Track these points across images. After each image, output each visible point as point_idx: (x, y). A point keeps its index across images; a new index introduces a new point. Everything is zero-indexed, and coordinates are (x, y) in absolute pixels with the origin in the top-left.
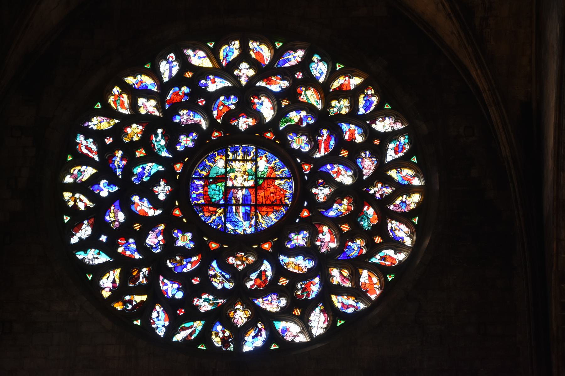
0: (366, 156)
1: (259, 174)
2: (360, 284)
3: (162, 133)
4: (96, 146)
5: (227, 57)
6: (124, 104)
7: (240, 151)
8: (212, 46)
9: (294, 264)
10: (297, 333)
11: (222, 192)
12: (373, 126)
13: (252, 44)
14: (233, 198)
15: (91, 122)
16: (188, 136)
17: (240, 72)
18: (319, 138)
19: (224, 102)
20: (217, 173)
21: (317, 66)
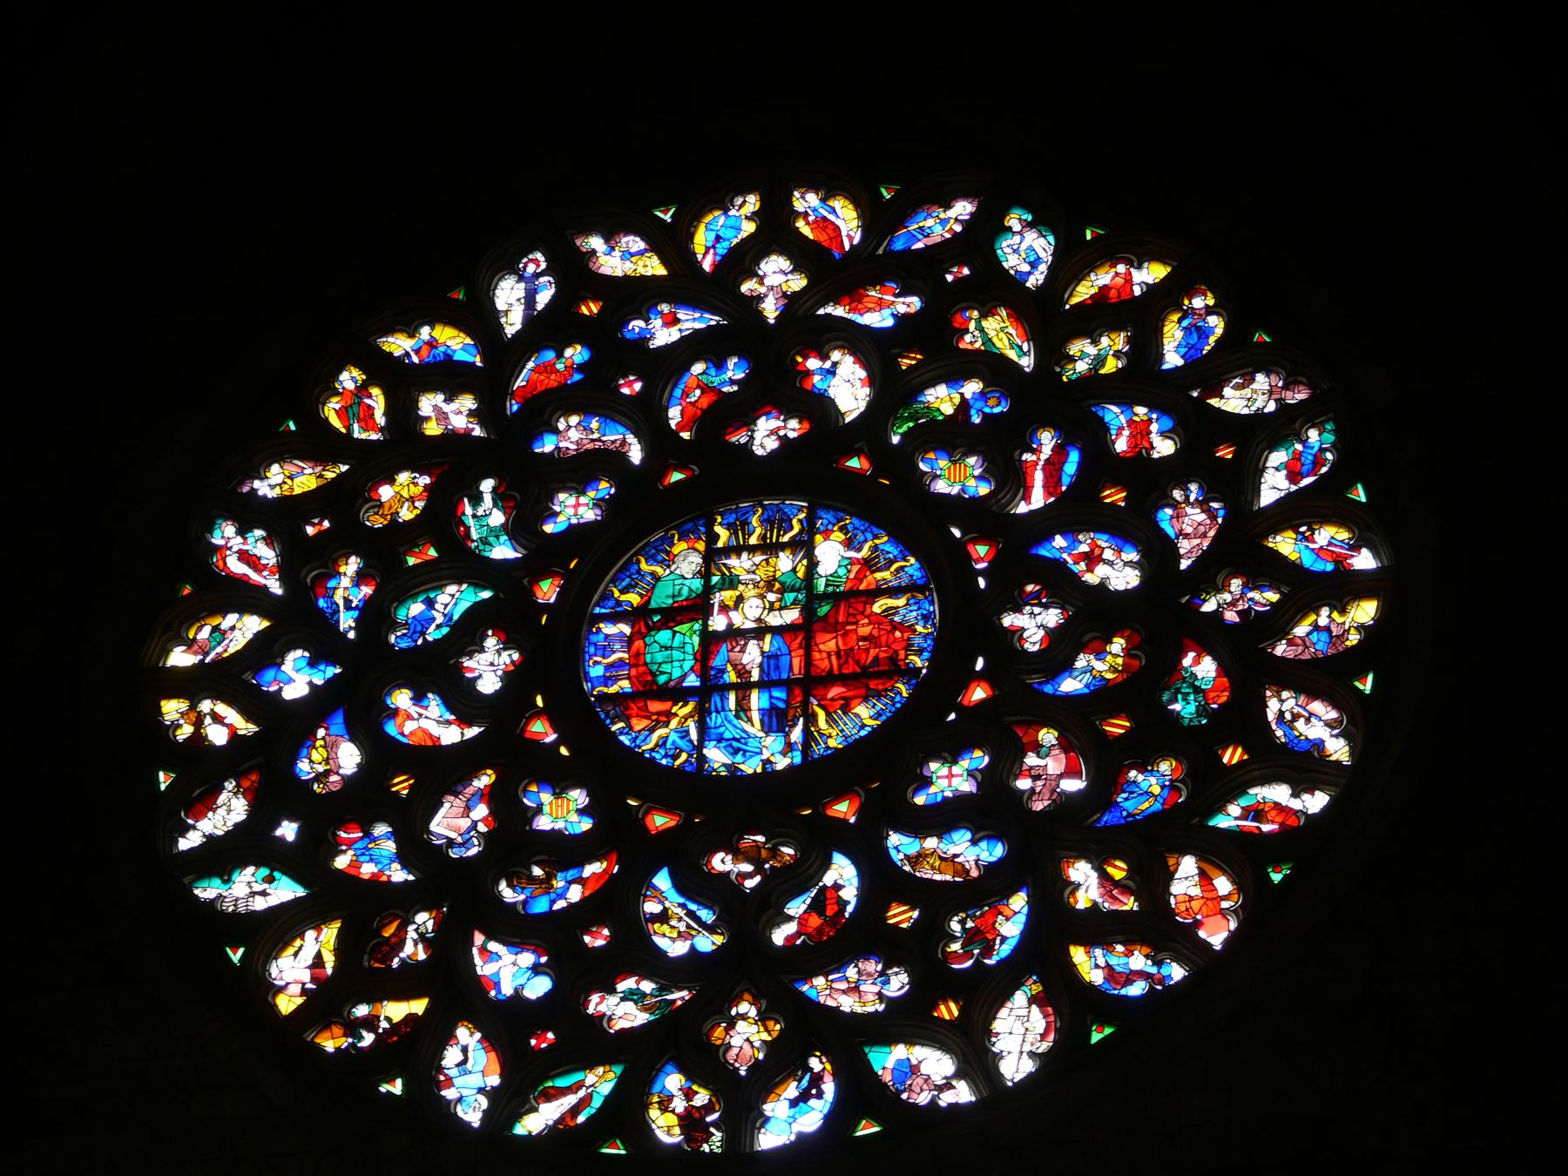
0: (1187, 497)
1: (821, 585)
2: (1172, 901)
3: (495, 491)
4: (275, 550)
5: (718, 245)
6: (373, 414)
7: (755, 521)
8: (667, 218)
9: (939, 855)
10: (946, 1078)
11: (691, 652)
12: (1214, 402)
13: (803, 198)
14: (729, 665)
15: (263, 478)
16: (583, 492)
17: (761, 283)
18: (1027, 457)
19: (704, 378)
20: (676, 593)
21: (1020, 243)
